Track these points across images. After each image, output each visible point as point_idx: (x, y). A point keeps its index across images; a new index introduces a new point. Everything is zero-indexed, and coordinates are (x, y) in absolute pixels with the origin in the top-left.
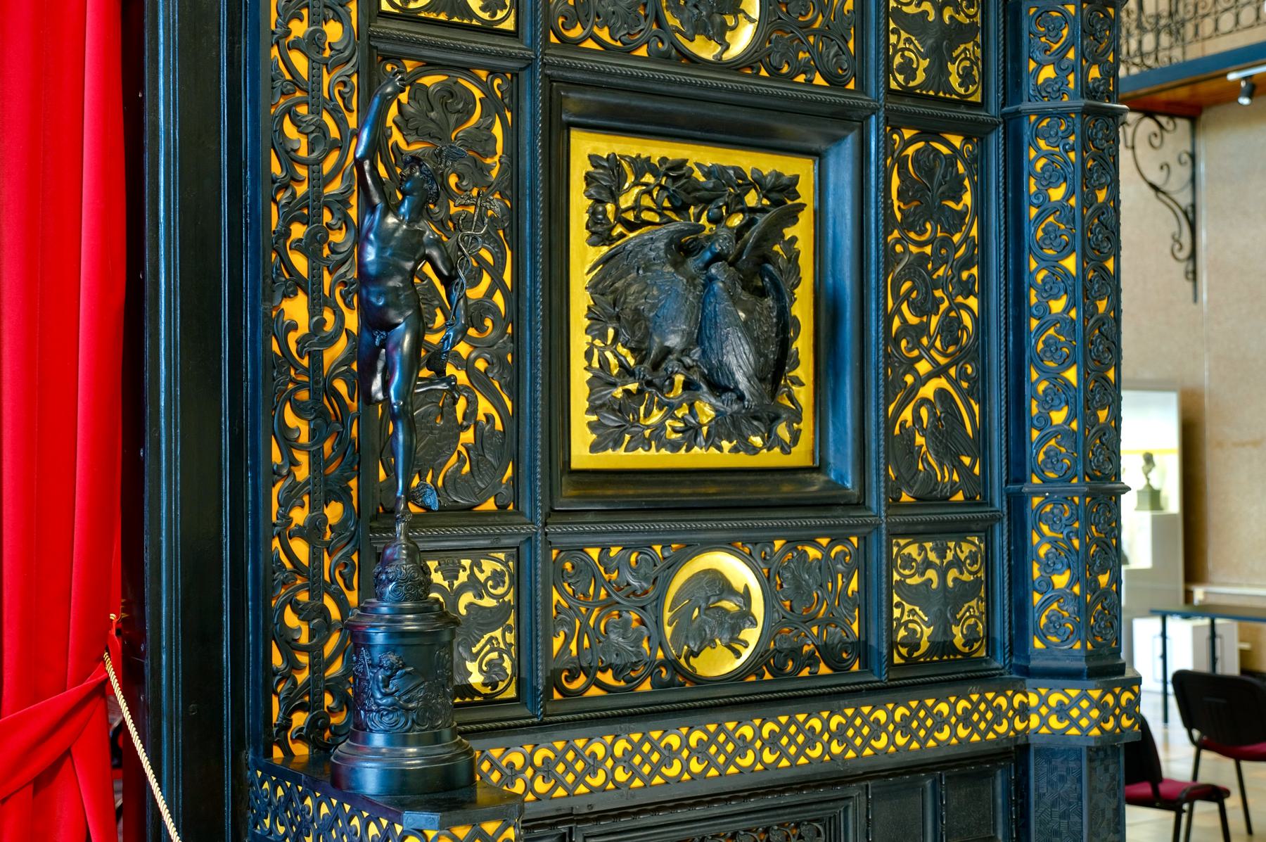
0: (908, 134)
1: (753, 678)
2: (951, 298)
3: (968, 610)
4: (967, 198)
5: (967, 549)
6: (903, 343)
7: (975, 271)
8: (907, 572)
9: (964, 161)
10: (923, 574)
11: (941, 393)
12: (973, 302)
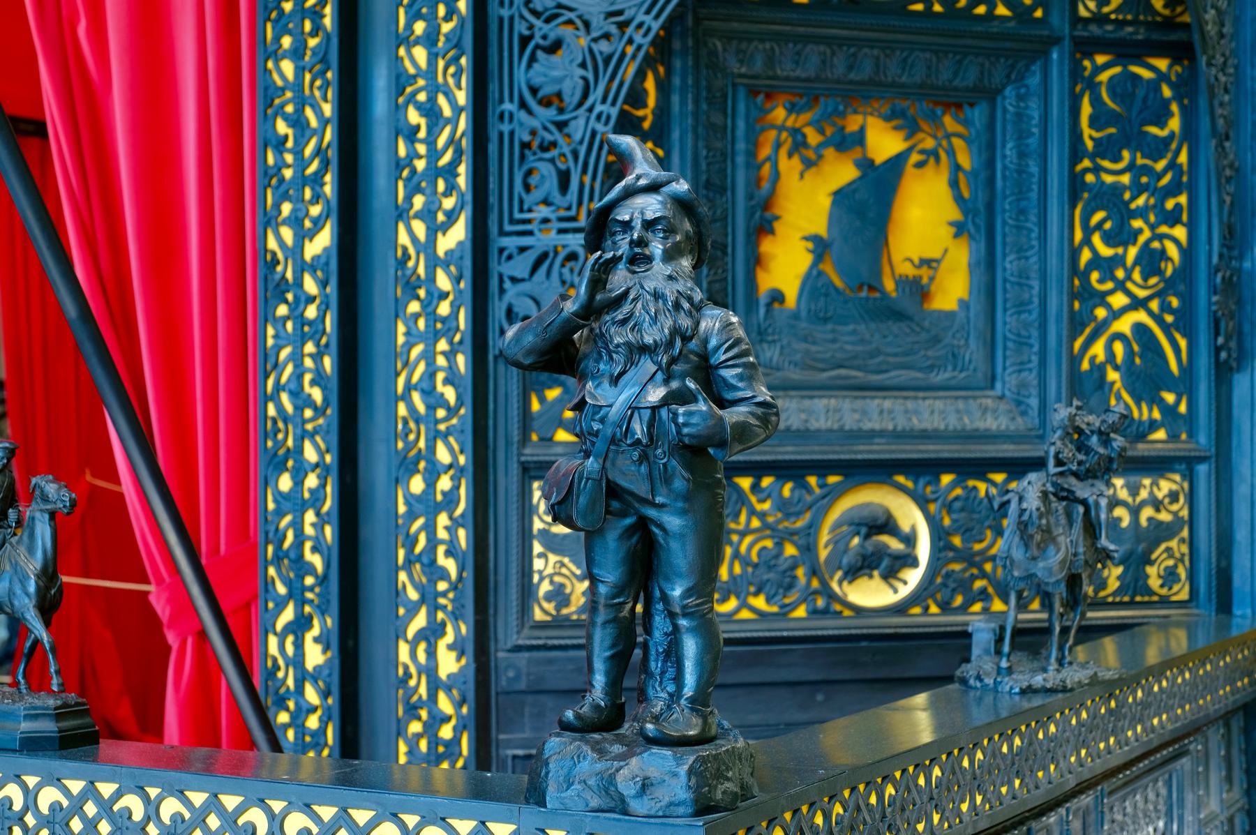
0: (1101, 59)
1: (917, 610)
2: (1152, 227)
3: (1168, 550)
4: (1175, 124)
5: (1165, 486)
6: (1095, 276)
7: (1183, 199)
9: (1172, 86)
11: (1139, 328)
12: (1180, 232)
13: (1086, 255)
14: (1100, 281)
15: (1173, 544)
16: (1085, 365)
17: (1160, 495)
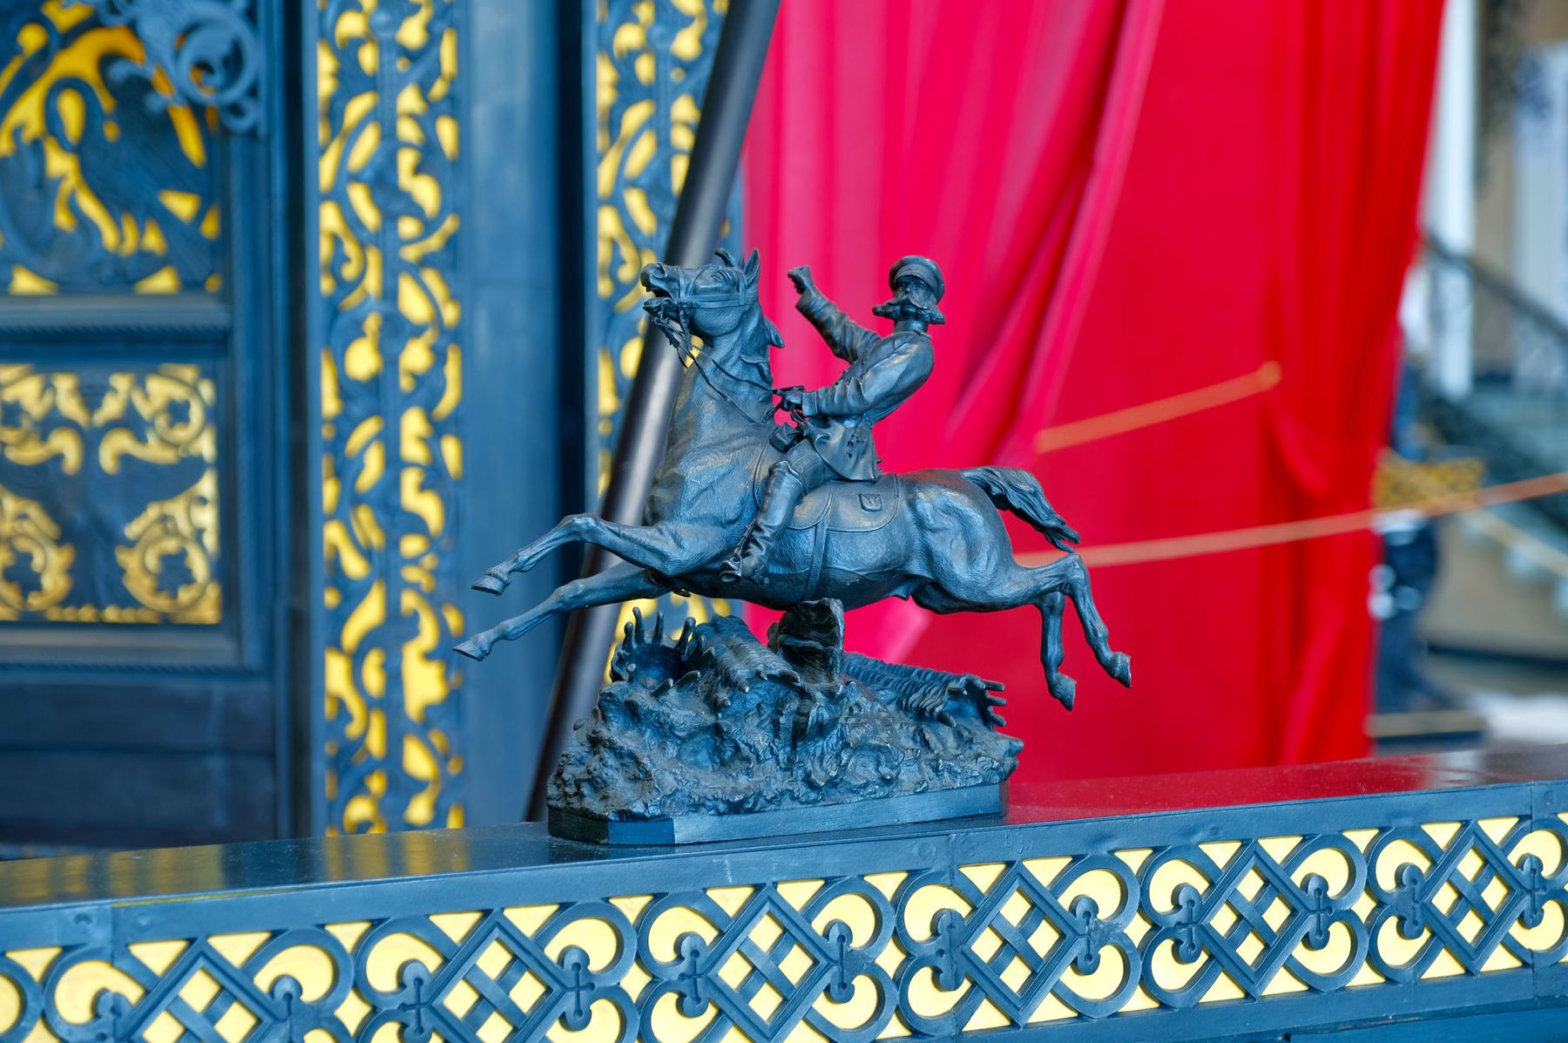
3: (164, 519)
5: (161, 389)
15: (177, 508)
17: (145, 410)
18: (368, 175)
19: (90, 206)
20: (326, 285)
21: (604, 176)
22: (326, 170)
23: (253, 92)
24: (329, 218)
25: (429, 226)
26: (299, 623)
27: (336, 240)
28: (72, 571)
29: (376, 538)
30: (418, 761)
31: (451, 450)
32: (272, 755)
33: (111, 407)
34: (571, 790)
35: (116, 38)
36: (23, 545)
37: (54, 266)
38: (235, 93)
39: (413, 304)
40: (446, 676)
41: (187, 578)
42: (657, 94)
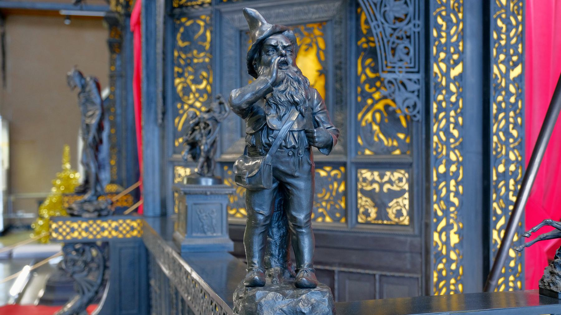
3: (397, 202)
5: (397, 175)
8: (364, 184)
10: (371, 185)
11: (387, 106)
13: (363, 78)
14: (370, 88)
15: (400, 200)
16: (363, 124)
17: (393, 179)
18: (444, 129)
19: (382, 136)
20: (434, 153)
21: (494, 128)
22: (435, 128)
23: (418, 112)
24: (435, 139)
25: (456, 140)
26: (427, 226)
27: (437, 144)
28: (377, 213)
29: (444, 207)
30: (453, 256)
31: (460, 188)
32: (421, 254)
33: (386, 179)
34: (546, 284)
35: (389, 101)
36: (367, 207)
37: (374, 149)
38: (415, 112)
39: (453, 157)
40: (459, 237)
41: (402, 215)
42: (506, 111)
